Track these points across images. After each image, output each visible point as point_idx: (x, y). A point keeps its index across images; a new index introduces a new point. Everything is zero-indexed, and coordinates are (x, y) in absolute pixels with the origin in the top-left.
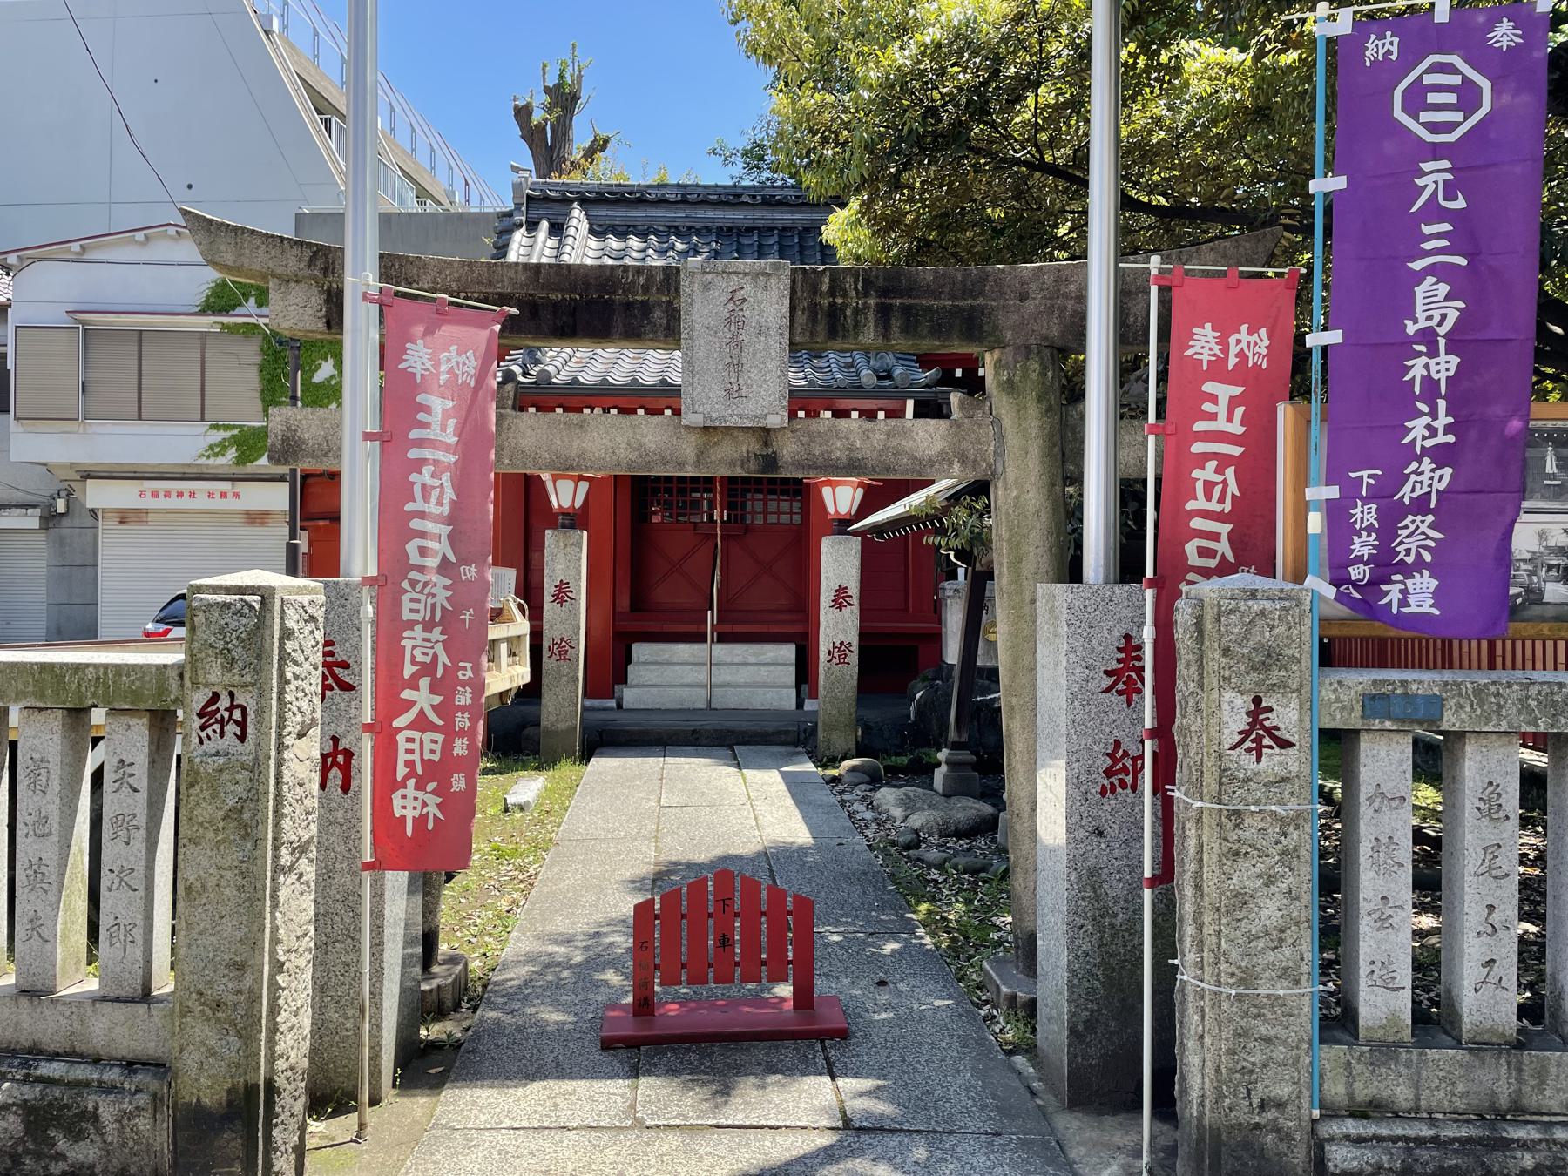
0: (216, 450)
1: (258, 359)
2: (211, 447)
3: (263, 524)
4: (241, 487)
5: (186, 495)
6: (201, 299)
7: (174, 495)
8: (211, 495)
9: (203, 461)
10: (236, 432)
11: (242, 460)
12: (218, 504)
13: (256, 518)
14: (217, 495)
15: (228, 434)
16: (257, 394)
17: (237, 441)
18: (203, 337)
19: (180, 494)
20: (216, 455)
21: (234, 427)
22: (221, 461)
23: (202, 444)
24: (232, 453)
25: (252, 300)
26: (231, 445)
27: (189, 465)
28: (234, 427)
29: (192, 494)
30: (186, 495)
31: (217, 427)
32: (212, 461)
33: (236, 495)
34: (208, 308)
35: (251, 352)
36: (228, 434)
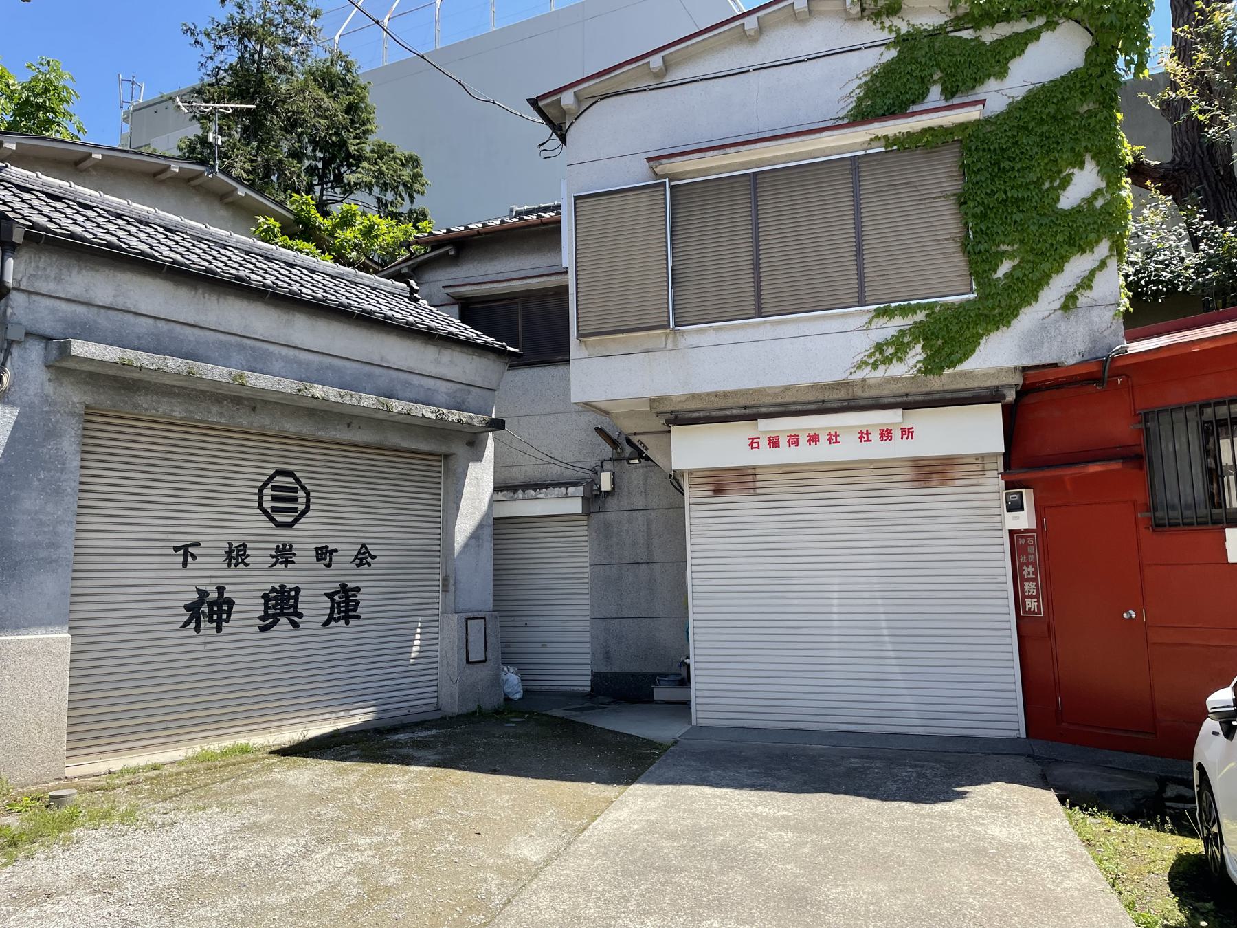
0: (884, 352)
1: (954, 185)
2: (879, 348)
3: (944, 482)
4: (921, 419)
5: (824, 438)
6: (845, 108)
7: (803, 440)
8: (864, 436)
9: (866, 373)
10: (920, 316)
11: (932, 365)
12: (878, 450)
13: (933, 471)
14: (875, 436)
15: (908, 321)
16: (955, 247)
17: (922, 333)
18: (855, 165)
19: (814, 439)
20: (888, 361)
21: (920, 307)
22: (897, 370)
23: (863, 343)
24: (916, 354)
25: (935, 93)
26: (916, 339)
27: (846, 384)
28: (911, 310)
29: (833, 438)
30: (824, 438)
31: (887, 313)
32: (880, 372)
33: (907, 433)
34: (861, 116)
35: (941, 176)
36: (908, 321)
